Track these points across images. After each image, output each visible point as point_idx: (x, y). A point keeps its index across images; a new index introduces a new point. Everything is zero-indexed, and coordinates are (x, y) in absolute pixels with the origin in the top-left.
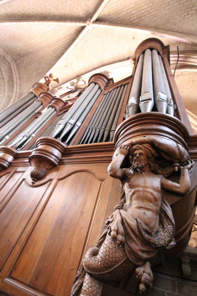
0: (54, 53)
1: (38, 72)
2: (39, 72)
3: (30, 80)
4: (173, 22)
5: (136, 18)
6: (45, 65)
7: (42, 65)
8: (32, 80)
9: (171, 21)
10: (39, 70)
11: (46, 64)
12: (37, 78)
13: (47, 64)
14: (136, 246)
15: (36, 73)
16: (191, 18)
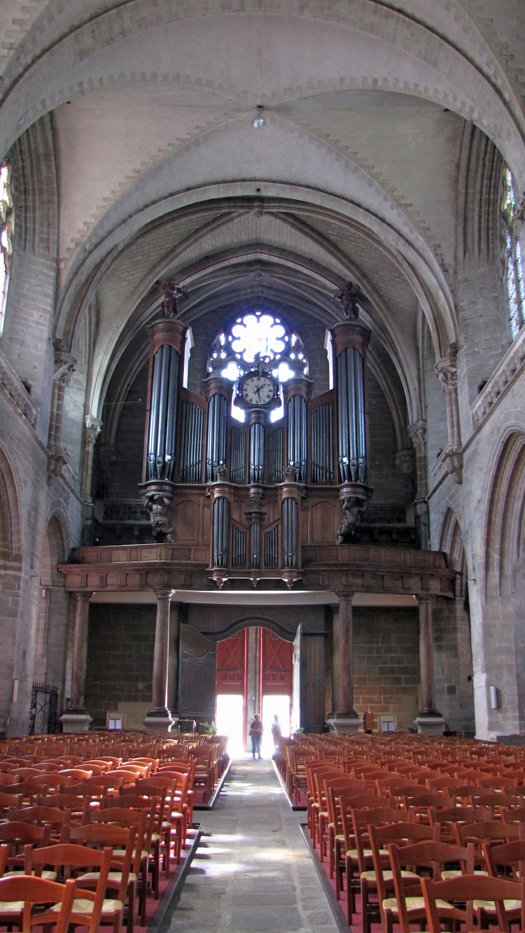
0: (173, 229)
1: (135, 260)
2: (138, 261)
3: (116, 274)
4: (382, 276)
5: (336, 234)
6: (152, 248)
7: (146, 248)
8: (122, 276)
9: (380, 273)
10: (136, 257)
11: (153, 246)
12: (134, 272)
13: (155, 247)
14: (352, 527)
15: (130, 261)
16: (400, 284)
